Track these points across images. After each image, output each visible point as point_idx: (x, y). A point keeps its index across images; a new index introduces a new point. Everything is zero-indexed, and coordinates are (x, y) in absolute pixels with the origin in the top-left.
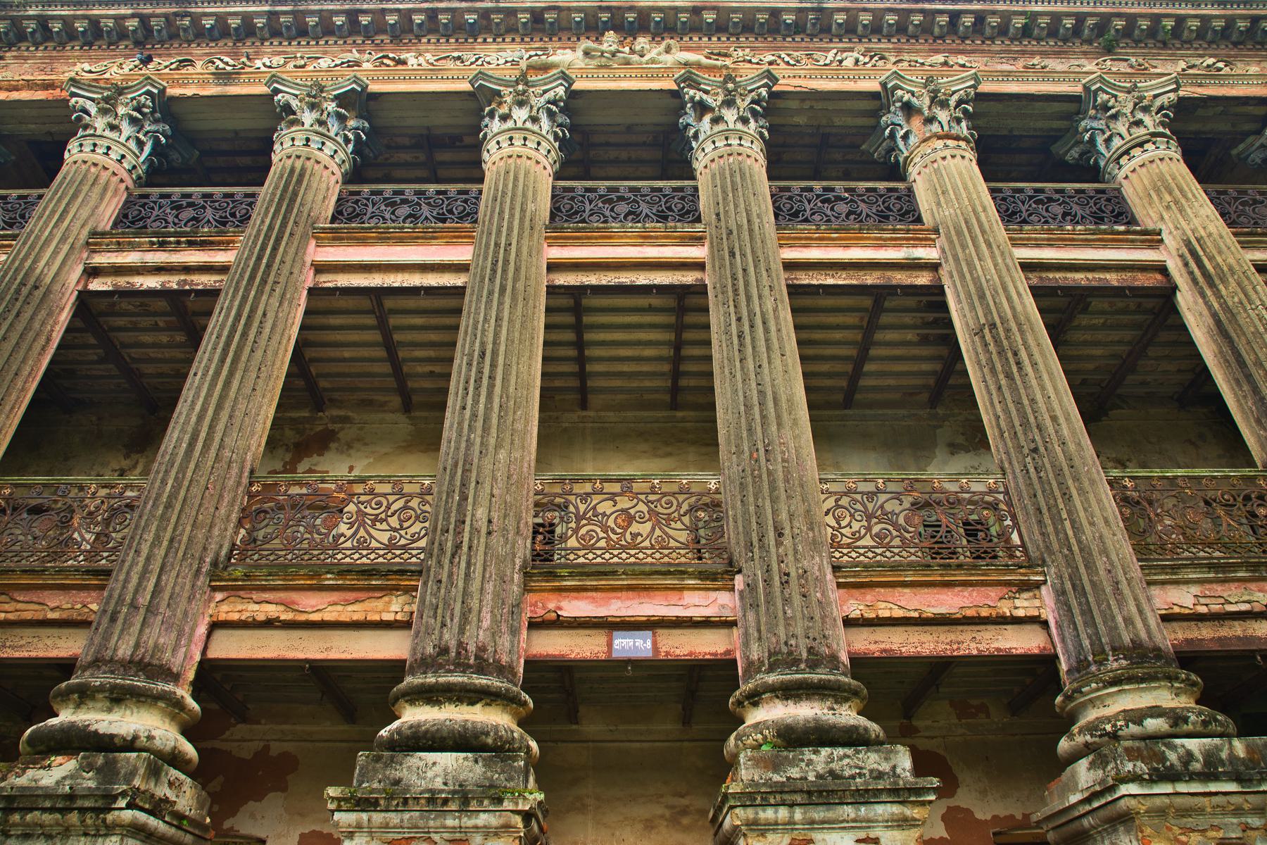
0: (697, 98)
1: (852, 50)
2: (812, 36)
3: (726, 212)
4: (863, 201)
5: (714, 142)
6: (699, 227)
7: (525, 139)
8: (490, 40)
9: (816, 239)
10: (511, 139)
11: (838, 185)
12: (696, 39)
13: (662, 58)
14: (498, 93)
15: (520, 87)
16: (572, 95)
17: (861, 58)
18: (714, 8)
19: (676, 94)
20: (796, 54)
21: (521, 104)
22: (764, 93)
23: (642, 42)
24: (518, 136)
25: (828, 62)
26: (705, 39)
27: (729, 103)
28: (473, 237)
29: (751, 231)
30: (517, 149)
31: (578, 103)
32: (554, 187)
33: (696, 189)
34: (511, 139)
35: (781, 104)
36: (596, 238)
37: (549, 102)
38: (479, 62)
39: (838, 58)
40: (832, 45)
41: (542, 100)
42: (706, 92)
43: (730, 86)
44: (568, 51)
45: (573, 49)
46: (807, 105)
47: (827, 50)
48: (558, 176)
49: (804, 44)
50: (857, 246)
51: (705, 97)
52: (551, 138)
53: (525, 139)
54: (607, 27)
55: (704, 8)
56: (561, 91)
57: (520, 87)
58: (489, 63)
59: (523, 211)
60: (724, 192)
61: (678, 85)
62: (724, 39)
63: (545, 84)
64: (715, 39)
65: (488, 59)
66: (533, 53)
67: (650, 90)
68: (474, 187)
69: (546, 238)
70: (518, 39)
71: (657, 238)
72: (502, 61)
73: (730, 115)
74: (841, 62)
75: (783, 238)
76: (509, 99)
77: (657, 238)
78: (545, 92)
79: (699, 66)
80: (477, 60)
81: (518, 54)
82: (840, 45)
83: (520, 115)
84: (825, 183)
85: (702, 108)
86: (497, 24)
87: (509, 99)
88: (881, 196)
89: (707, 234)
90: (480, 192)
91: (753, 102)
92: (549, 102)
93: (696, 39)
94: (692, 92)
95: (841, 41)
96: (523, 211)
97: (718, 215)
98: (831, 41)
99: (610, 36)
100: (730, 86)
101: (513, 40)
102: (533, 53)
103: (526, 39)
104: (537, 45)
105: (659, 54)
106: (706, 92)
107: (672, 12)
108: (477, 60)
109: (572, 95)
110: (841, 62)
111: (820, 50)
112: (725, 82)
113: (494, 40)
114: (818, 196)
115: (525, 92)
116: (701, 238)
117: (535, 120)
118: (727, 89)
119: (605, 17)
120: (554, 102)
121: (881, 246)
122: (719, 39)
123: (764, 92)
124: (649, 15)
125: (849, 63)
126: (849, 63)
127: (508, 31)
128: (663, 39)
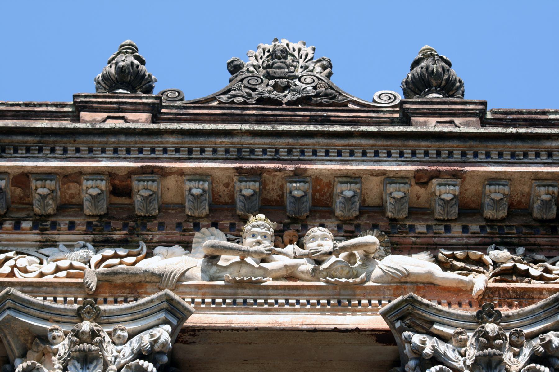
0: (428, 350)
14: (43, 338)
15: (86, 326)
16: (184, 335)
18: (455, 175)
19: (382, 337)
31: (197, 350)
41: (127, 349)
44: (177, 249)
45: (187, 246)
51: (442, 347)
55: (437, 175)
56: (164, 333)
57: (86, 326)
58: (25, 270)
61: (391, 324)
66: (109, 252)
67: (336, 330)
76: (62, 347)
79: (427, 285)
86: (43, 197)
87: (62, 347)
94: (417, 339)
100: (491, 328)
104: (117, 236)
106: (444, 339)
107: (376, 180)
109: (184, 335)
112: (480, 319)
113: (34, 227)
115: (94, 334)
118: (485, 334)
119: (248, 188)
122: (465, 229)
124: (330, 185)
127: (62, 208)
128: (358, 227)
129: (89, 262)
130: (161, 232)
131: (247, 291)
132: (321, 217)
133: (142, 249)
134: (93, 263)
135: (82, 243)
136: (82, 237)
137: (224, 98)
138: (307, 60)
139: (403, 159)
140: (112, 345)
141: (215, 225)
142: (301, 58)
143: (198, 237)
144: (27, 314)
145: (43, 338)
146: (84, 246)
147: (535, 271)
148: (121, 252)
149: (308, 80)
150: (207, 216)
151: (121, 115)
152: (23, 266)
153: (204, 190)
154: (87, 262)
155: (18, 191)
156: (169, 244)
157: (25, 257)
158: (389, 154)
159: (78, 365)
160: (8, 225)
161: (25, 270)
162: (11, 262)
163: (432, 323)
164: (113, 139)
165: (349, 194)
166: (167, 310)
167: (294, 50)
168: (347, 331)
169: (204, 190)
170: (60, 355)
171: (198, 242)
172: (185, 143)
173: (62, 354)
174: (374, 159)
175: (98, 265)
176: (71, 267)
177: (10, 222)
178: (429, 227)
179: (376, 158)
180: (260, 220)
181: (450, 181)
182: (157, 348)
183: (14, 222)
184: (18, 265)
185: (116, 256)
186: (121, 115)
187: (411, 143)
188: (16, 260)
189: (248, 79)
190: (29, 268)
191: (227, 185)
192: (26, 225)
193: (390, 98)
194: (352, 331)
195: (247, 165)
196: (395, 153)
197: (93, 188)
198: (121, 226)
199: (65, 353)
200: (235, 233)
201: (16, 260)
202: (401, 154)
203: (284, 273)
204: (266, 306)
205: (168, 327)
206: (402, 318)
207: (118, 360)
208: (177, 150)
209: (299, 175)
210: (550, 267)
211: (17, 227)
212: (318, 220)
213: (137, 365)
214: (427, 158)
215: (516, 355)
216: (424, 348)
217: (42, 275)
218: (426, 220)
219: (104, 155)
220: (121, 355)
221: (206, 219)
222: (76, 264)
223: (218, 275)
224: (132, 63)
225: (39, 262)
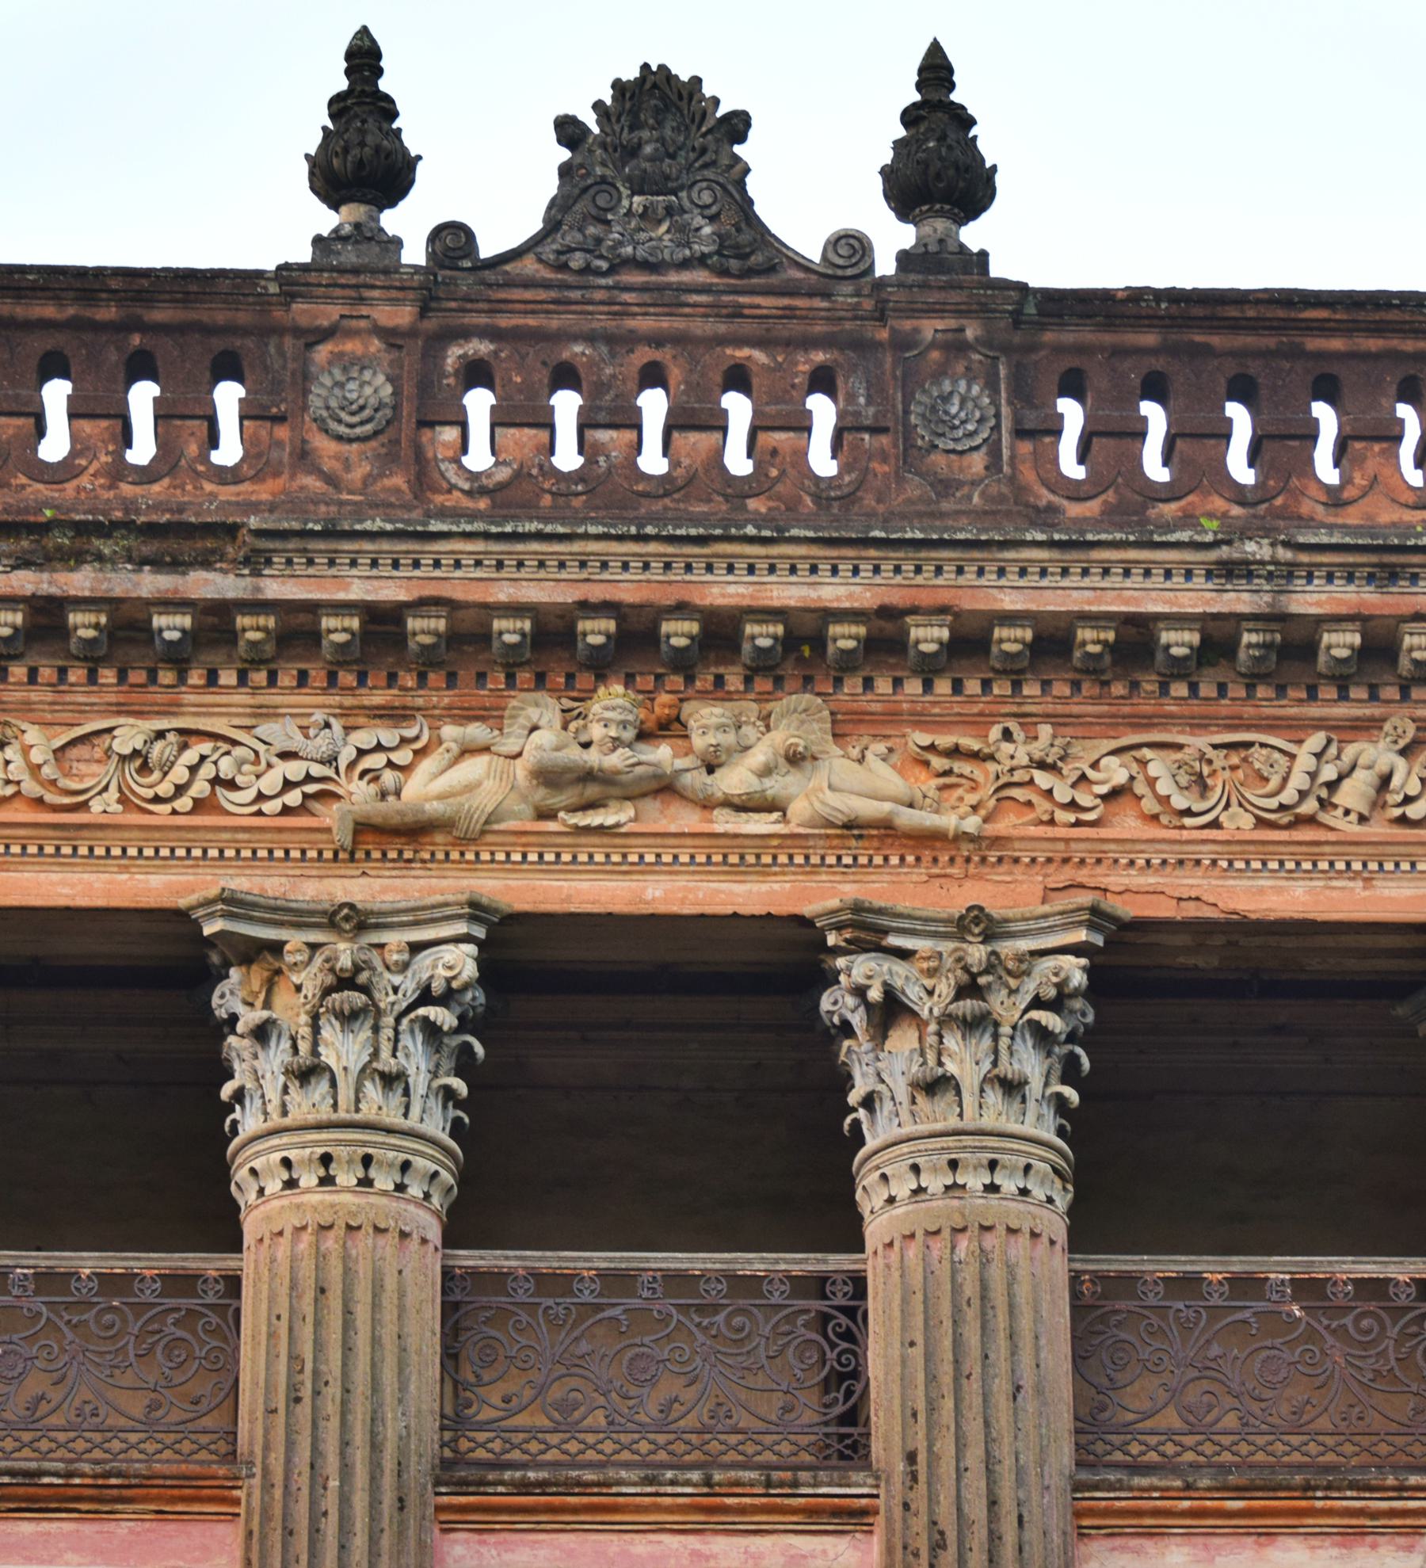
1: (1367, 727)
2: (1253, 679)
3: (933, 1458)
4: (1340, 1333)
5: (916, 1169)
6: (859, 1486)
7: (367, 1161)
8: (228, 678)
9: (1184, 1514)
10: (326, 1160)
11: (1278, 1268)
12: (883, 686)
13: (774, 786)
14: (276, 948)
15: (345, 953)
17: (1401, 764)
18: (943, 610)
20: (1200, 742)
21: (348, 1018)
22: (1078, 979)
23: (707, 720)
24: (345, 1147)
25: (1288, 796)
26: (913, 687)
27: (972, 1025)
28: (236, 1502)
29: (994, 1537)
30: (345, 1198)
32: (447, 1273)
33: (859, 1283)
34: (326, 1160)
35: (1130, 936)
36: (575, 1510)
37: (425, 997)
38: (200, 788)
39: (1329, 773)
40: (1314, 711)
41: (409, 985)
42: (904, 954)
43: (977, 953)
44: (477, 731)
46: (1219, 940)
47: (1297, 729)
48: (459, 1229)
49: (1225, 707)
50: (1292, 1531)
51: (899, 973)
52: (436, 1124)
53: (367, 1161)
54: (601, 665)
55: (914, 610)
59: (375, 1447)
60: (931, 1378)
62: (973, 686)
63: (416, 923)
64: (943, 687)
65: (226, 767)
66: (364, 738)
67: (735, 915)
68: (210, 1264)
69: (439, 1509)
70: (318, 677)
71: (742, 1510)
72: (270, 782)
73: (964, 1059)
74: (1332, 786)
75: (1091, 1513)
77: (742, 1510)
78: (416, 948)
79: (884, 831)
80: (193, 769)
81: (321, 744)
82: (1342, 711)
83: (343, 1050)
84: (1239, 1264)
85: (890, 1011)
87: (311, 979)
88: (1398, 1312)
89: (880, 1502)
90: (233, 1284)
91: (1037, 1003)
92: (425, 997)
93: (883, 686)
94: (860, 968)
95: (1343, 696)
96: (375, 1447)
97: (911, 1458)
98: (1312, 694)
99: (612, 703)
101: (303, 678)
102: (364, 738)
103: (347, 678)
104: (378, 698)
105: (766, 771)
106: (904, 954)
108: (193, 769)
110: (1332, 786)
111: (1272, 725)
113: (243, 679)
114: (1215, 1312)
116: (864, 1512)
117: (391, 1080)
118: (966, 969)
119: (596, 631)
120: (447, 998)
121: (1361, 1533)
122: (957, 687)
123: (1075, 970)
125: (1354, 793)
126: (1354, 793)
128: (778, 681)
129: (336, 759)
130: (451, 693)
131: (596, 840)
132: (717, 664)
133: (421, 730)
134: (343, 764)
135: (319, 716)
136: (320, 699)
137: (548, 250)
138: (704, 129)
139: (857, 580)
140: (387, 975)
141: (540, 681)
142: (693, 121)
143: (514, 708)
144: (251, 919)
145: (276, 948)
146: (327, 725)
147: (1063, 794)
148: (389, 737)
149: (706, 197)
150: (528, 662)
151: (365, 311)
152: (230, 777)
153: (523, 635)
154: (331, 760)
155: (211, 620)
156: (466, 716)
157: (228, 753)
158: (835, 571)
159: (337, 1024)
160: (196, 678)
161: (231, 785)
162: (208, 771)
163: (886, 932)
164: (368, 546)
165: (764, 643)
166: (473, 919)
167: (681, 97)
168: (753, 916)
169: (523, 635)
170: (306, 997)
171: (512, 717)
172: (491, 553)
173: (310, 996)
174: (808, 580)
175: (352, 765)
176: (309, 778)
177: (200, 671)
178: (897, 682)
179: (814, 578)
180: (617, 696)
181: (934, 619)
182: (455, 985)
183: (205, 672)
184: (222, 776)
185: (379, 748)
186: (365, 311)
187: (872, 553)
188: (215, 763)
189: (592, 191)
190: (239, 780)
191: (562, 617)
192: (228, 678)
193: (855, 251)
194: (761, 916)
195: (597, 593)
196: (845, 567)
197: (338, 629)
198: (384, 683)
199: (314, 995)
200: (575, 694)
201: (215, 763)
202: (856, 571)
203: (654, 785)
204: (624, 868)
205: (471, 949)
206: (839, 927)
207: (396, 1007)
208: (478, 563)
209: (681, 609)
210: (1091, 774)
211: (212, 678)
212: (713, 670)
213: (426, 1019)
214: (899, 579)
215: (1012, 992)
216: (869, 987)
217: (261, 797)
218: (893, 667)
219: (354, 572)
220: (400, 995)
221: (527, 668)
222: (317, 770)
223: (549, 802)
224: (378, 149)
225: (252, 756)
